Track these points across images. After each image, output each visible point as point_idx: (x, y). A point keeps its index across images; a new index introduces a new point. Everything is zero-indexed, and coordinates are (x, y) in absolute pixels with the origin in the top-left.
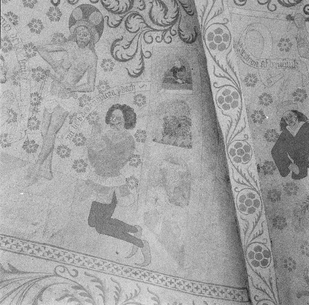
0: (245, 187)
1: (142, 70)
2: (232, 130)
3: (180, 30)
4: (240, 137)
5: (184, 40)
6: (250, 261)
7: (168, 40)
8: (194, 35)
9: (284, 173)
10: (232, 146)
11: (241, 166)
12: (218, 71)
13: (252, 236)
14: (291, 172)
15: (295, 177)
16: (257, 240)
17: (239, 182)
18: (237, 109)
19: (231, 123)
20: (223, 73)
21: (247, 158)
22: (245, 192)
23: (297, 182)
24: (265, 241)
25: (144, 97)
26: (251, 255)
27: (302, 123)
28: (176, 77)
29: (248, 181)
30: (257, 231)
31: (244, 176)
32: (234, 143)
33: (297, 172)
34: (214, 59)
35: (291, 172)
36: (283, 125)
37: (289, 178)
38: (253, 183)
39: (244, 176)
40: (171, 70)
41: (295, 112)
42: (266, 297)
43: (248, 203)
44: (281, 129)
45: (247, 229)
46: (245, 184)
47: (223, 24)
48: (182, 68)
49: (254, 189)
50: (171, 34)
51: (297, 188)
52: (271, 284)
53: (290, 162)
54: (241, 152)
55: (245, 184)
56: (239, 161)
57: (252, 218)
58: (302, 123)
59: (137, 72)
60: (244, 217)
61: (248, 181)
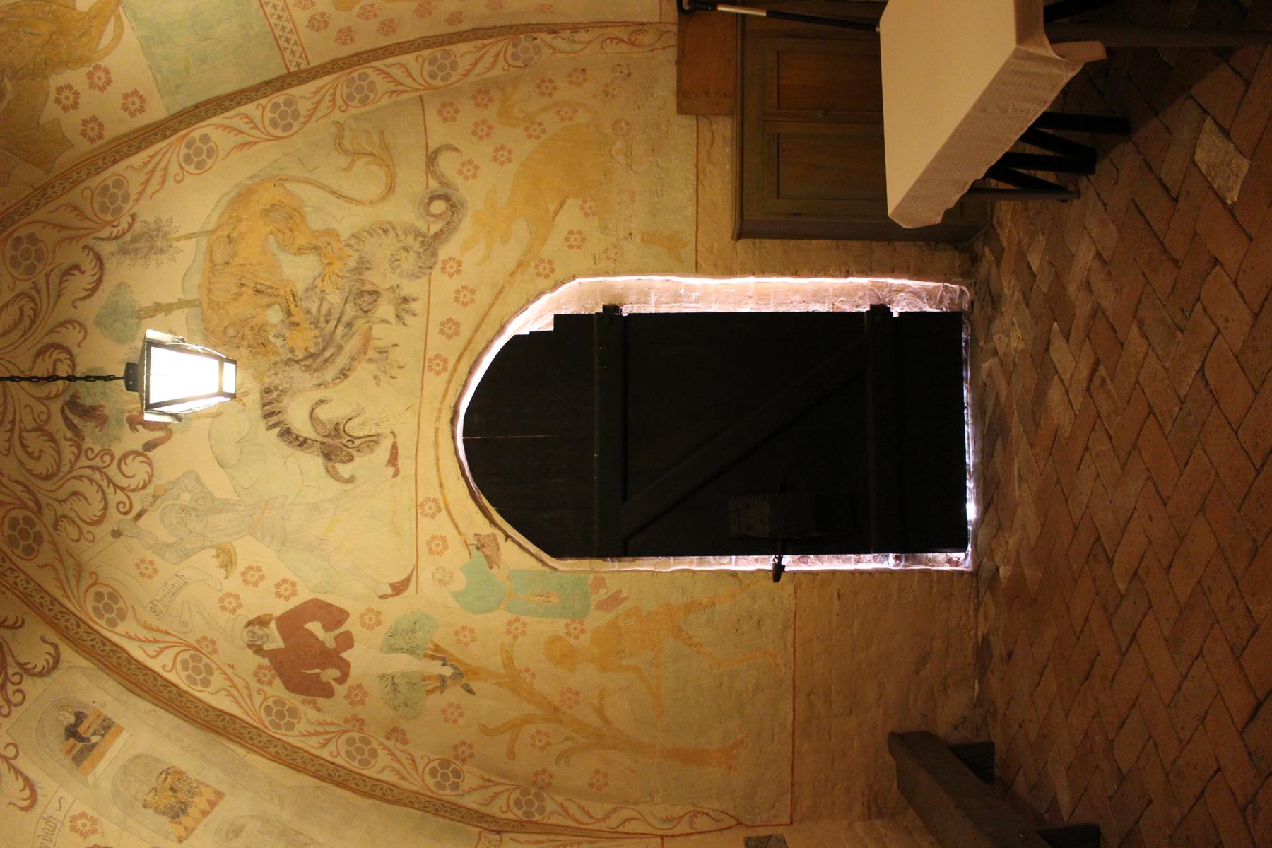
0: (334, 741)
1: (29, 784)
2: (243, 703)
3: (21, 665)
4: (258, 700)
5: (41, 674)
6: (448, 791)
7: (19, 697)
8: (52, 651)
9: (328, 692)
10: (266, 720)
11: (302, 727)
12: (152, 649)
13: (413, 773)
14: (333, 682)
15: (341, 680)
16: (420, 771)
17: (324, 745)
18: (217, 673)
19: (231, 695)
20: (156, 647)
21: (293, 712)
22: (343, 749)
23: (351, 681)
24: (426, 759)
25: (83, 815)
26: (440, 786)
27: (273, 625)
28: (83, 740)
29: (327, 733)
30: (407, 763)
31: (317, 733)
32: (263, 713)
33: (337, 673)
34: (129, 637)
35: (333, 682)
36: (258, 650)
37: (340, 690)
38: (333, 729)
39: (317, 733)
40: (67, 738)
41: (250, 623)
42: (506, 794)
43: (360, 751)
44: (264, 657)
45: (398, 773)
46: (330, 740)
47: (94, 584)
48: (80, 717)
49: (346, 732)
50: (14, 684)
51: (359, 686)
52: (489, 780)
53: (318, 675)
54: (281, 715)
55: (330, 740)
56: (290, 727)
57: (383, 759)
58: (273, 625)
59: (27, 793)
60: (378, 767)
61: (327, 733)
